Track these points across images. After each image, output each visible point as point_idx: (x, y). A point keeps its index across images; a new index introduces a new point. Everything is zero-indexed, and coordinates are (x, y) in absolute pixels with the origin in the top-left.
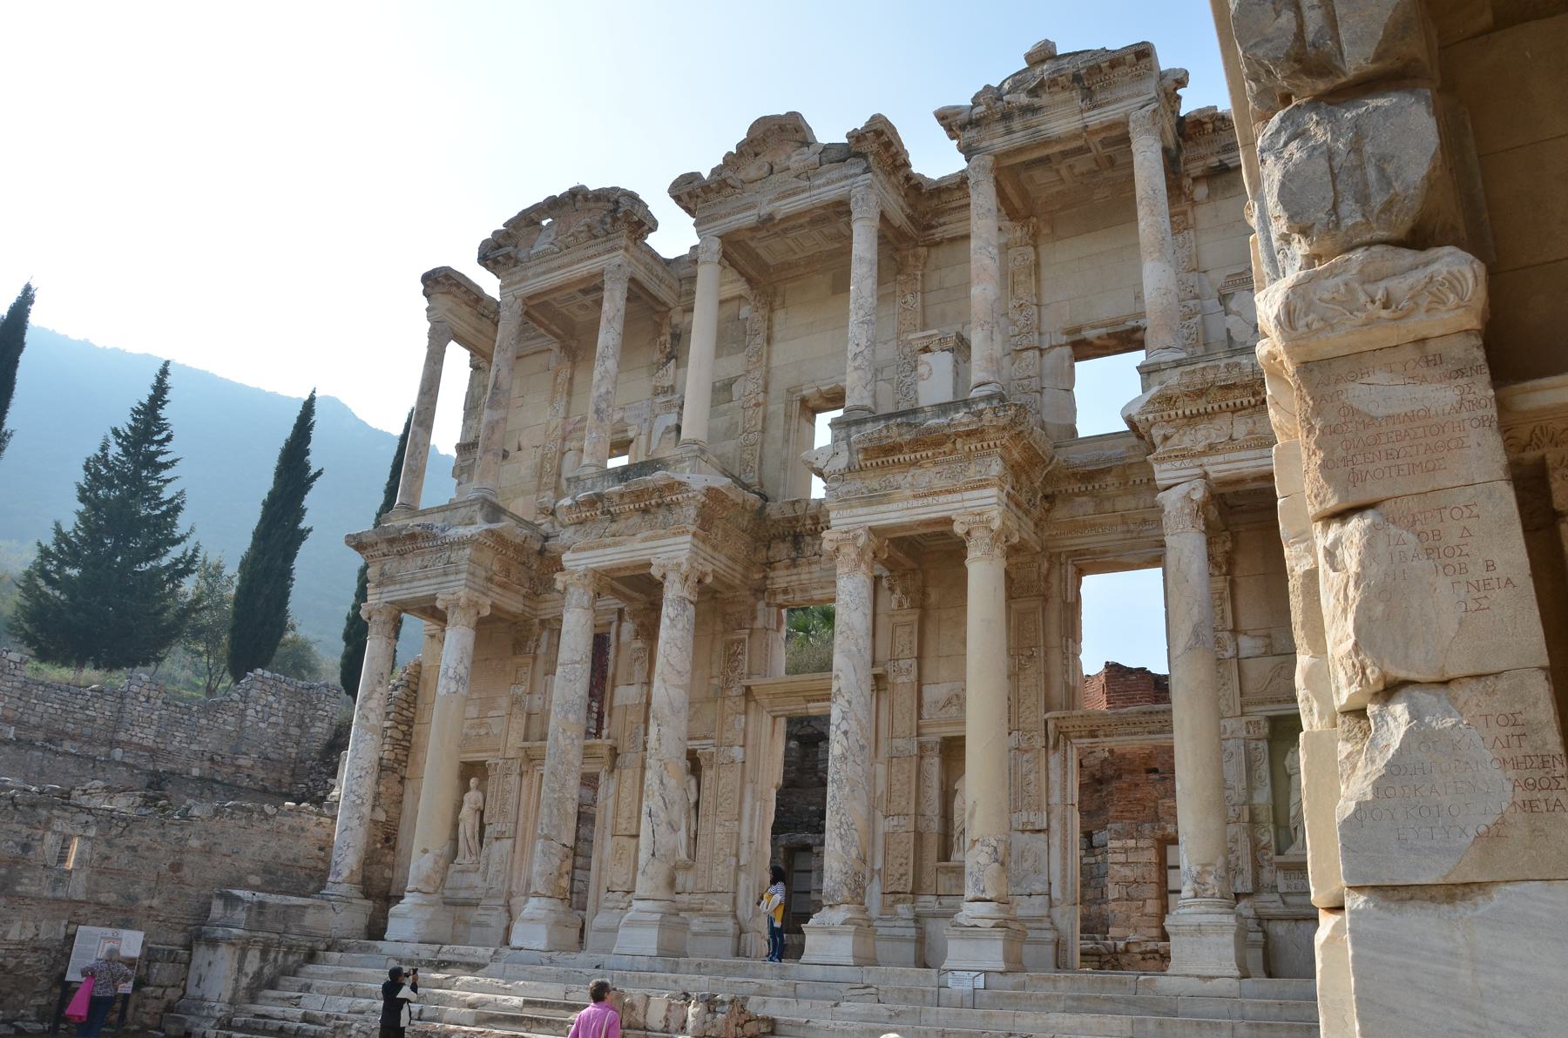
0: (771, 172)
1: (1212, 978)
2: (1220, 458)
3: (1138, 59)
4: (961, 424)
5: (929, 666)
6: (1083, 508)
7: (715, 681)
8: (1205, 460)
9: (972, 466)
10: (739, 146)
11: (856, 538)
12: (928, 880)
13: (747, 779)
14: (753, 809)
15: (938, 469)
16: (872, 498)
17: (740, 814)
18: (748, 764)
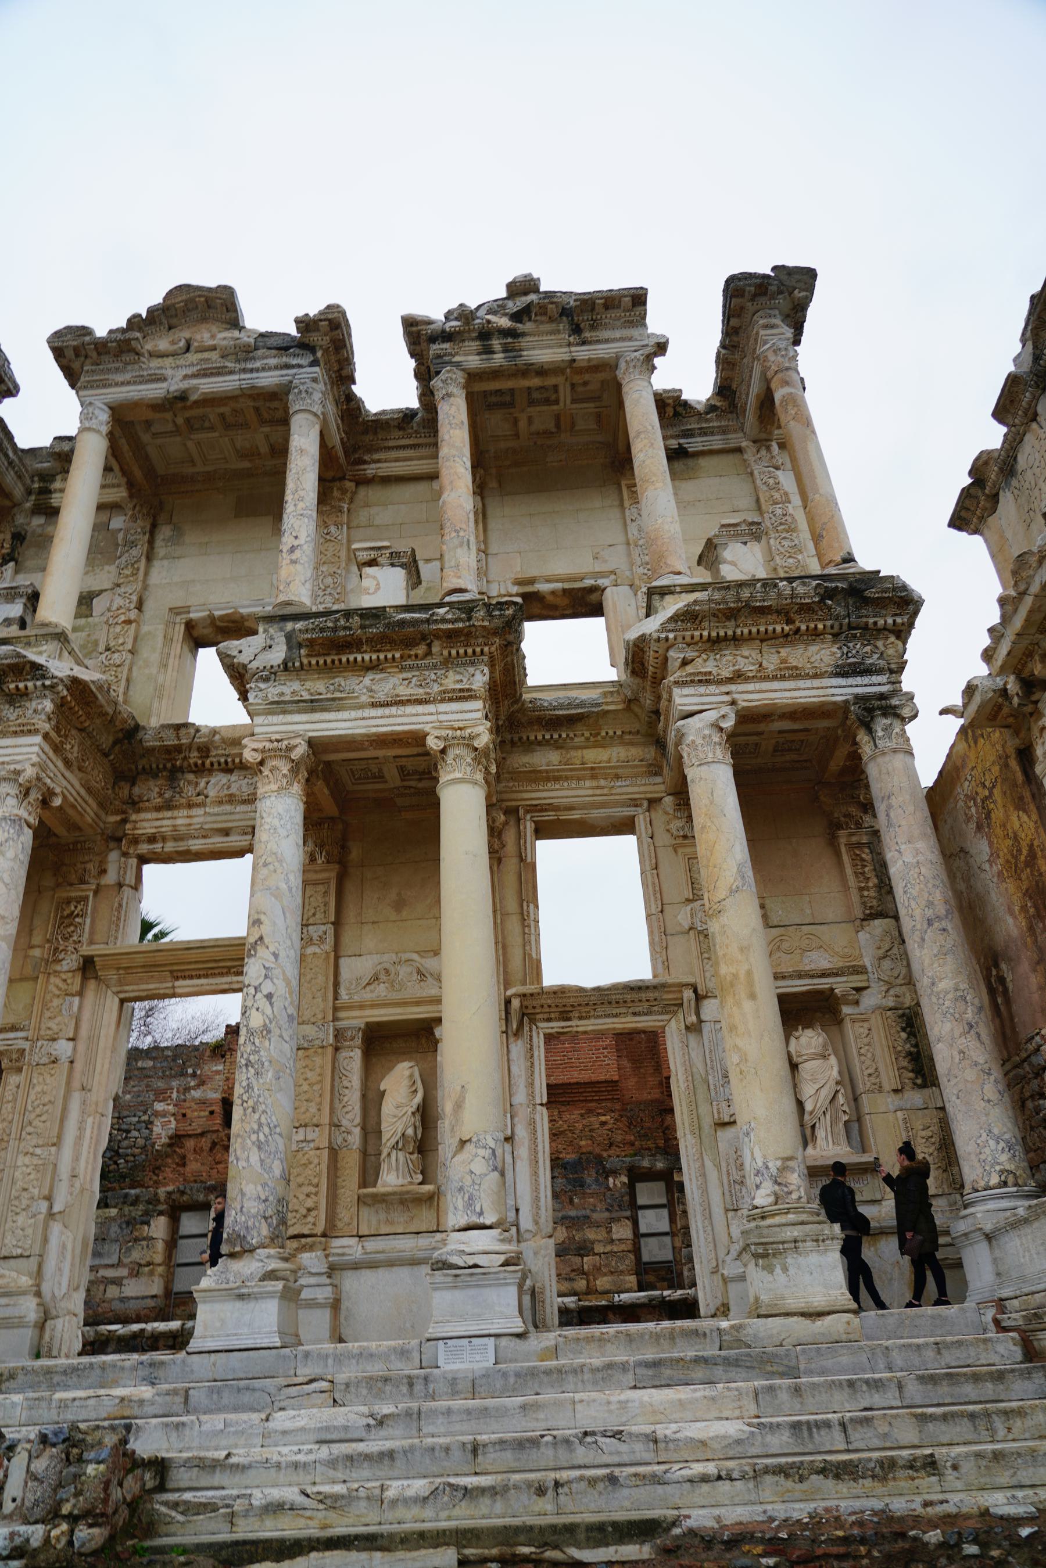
0: (188, 350)
1: (821, 1314)
2: (750, 687)
3: (634, 305)
4: (444, 620)
5: (348, 936)
6: (546, 759)
7: (37, 953)
8: (732, 687)
9: (451, 673)
10: (151, 311)
11: (290, 749)
12: (345, 1214)
13: (76, 1084)
14: (81, 1129)
15: (405, 675)
16: (314, 705)
17: (60, 1137)
18: (78, 1066)
